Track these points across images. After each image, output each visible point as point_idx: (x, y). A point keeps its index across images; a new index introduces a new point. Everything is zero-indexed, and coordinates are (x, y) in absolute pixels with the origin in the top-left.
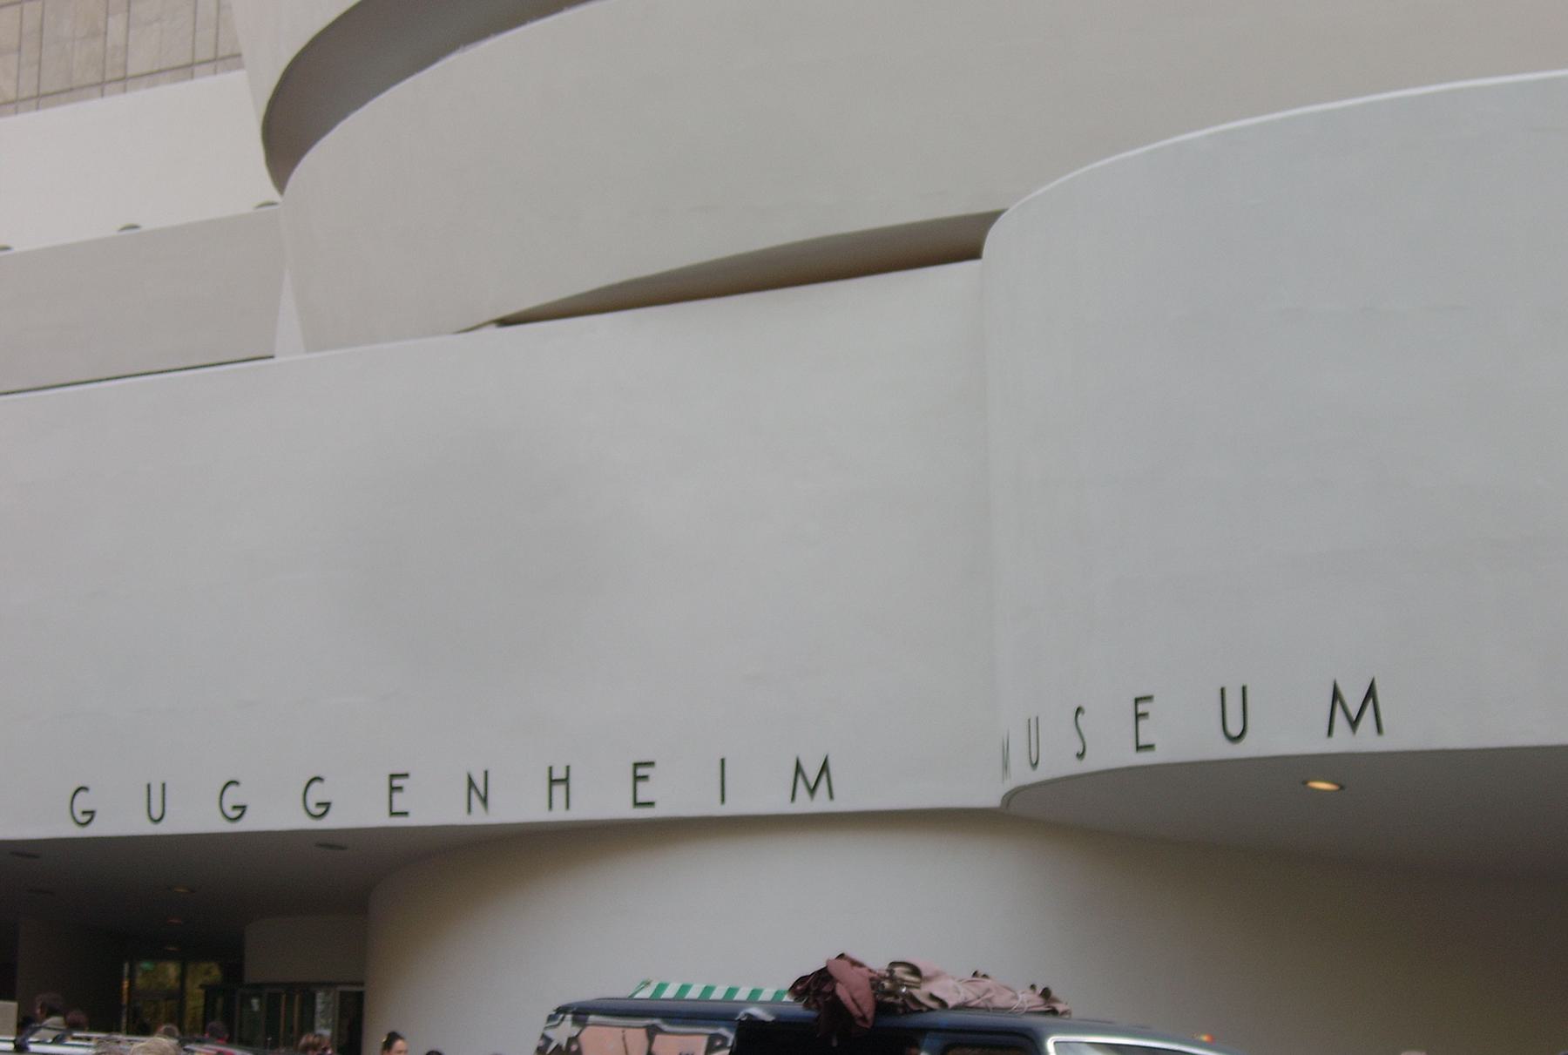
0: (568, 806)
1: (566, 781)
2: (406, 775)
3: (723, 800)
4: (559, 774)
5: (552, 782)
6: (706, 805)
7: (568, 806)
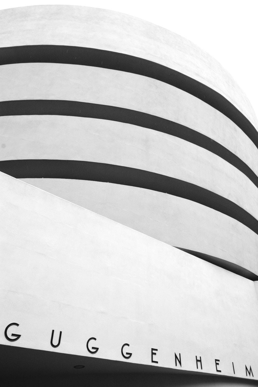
0: (202, 368)
1: (200, 361)
2: (157, 350)
4: (199, 359)
5: (197, 361)
7: (202, 368)
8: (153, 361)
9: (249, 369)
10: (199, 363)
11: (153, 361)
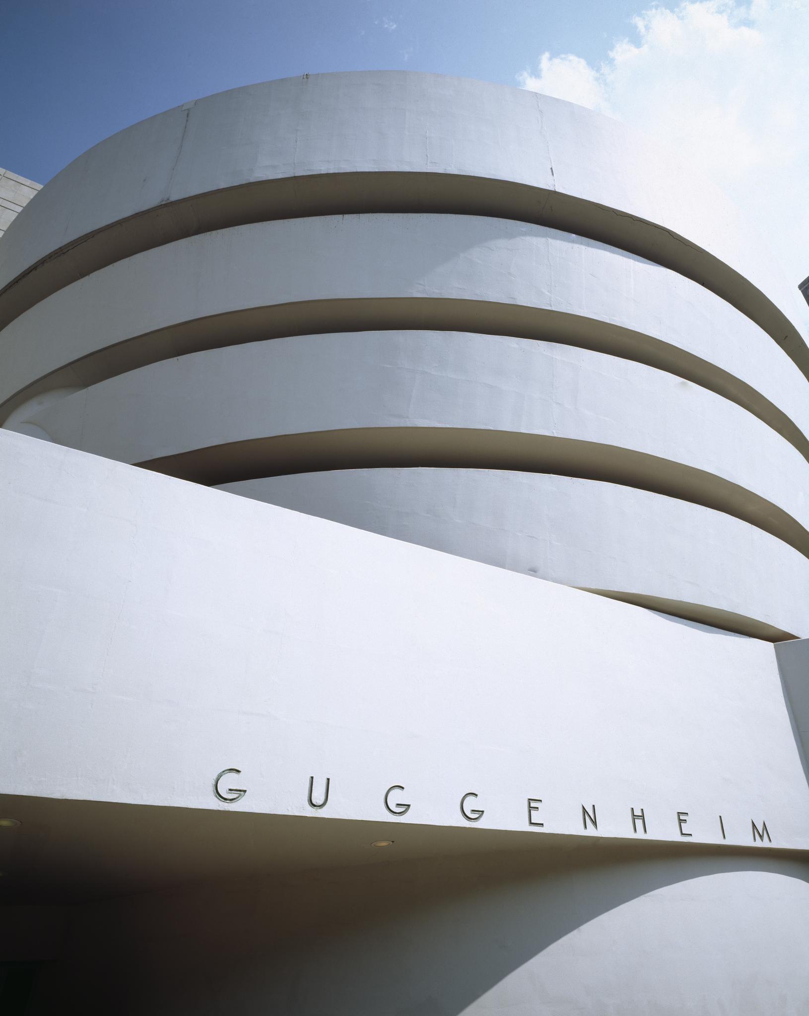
1: (642, 817)
3: (645, 831)
4: (638, 812)
6: (715, 839)
7: (645, 831)
8: (531, 823)
9: (760, 828)
10: (639, 823)
11: (531, 823)
